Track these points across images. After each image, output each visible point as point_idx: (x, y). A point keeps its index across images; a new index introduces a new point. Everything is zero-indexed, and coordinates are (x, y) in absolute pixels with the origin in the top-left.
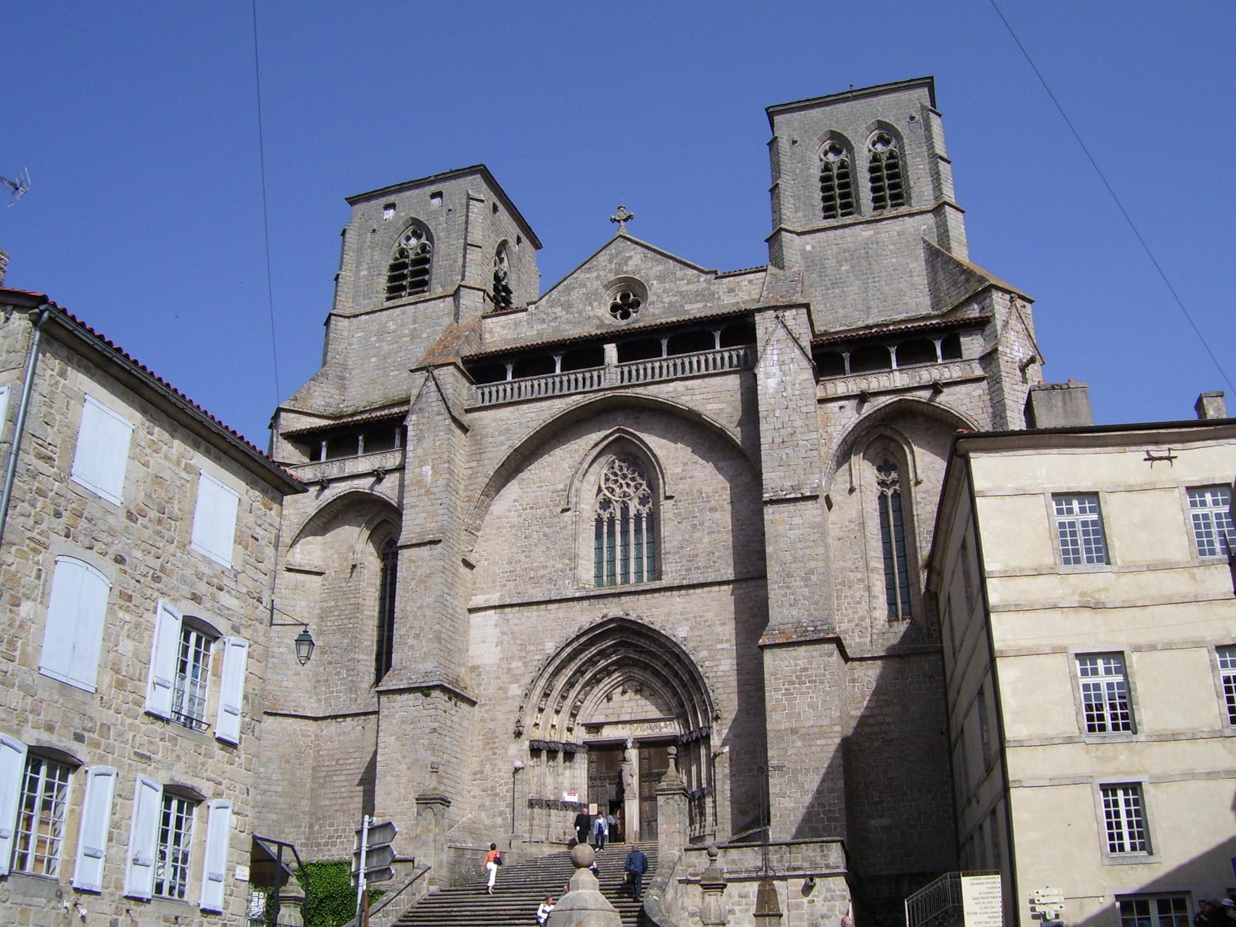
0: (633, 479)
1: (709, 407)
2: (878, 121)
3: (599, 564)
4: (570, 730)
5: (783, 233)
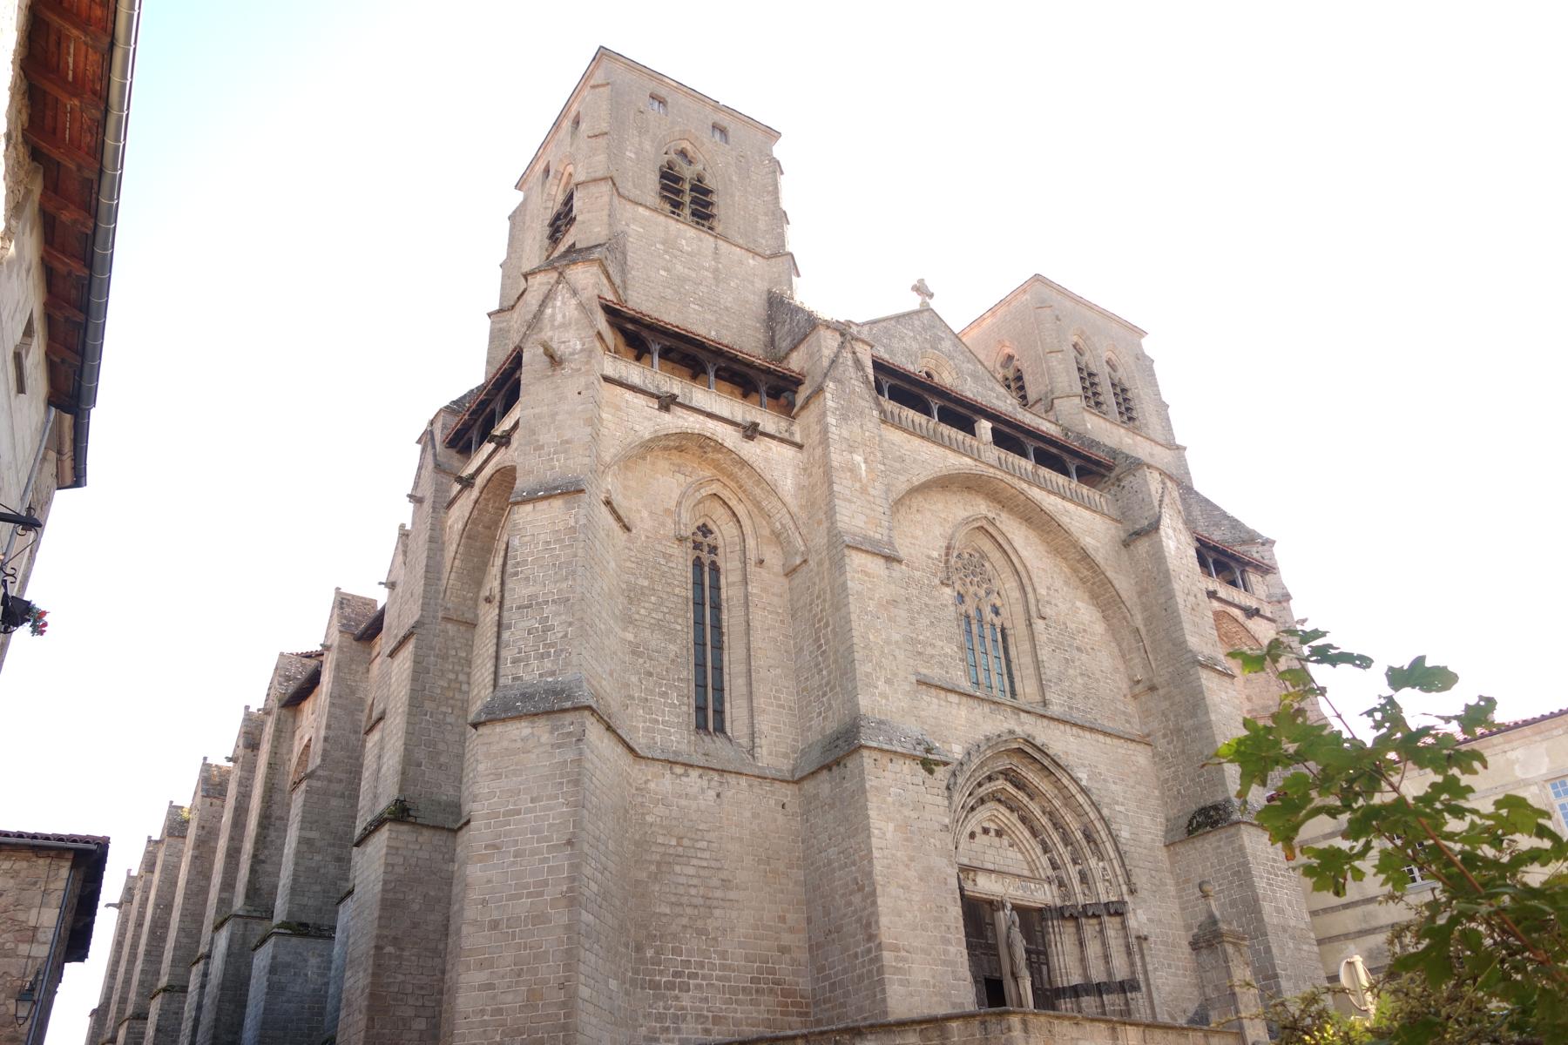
1: (1088, 539)
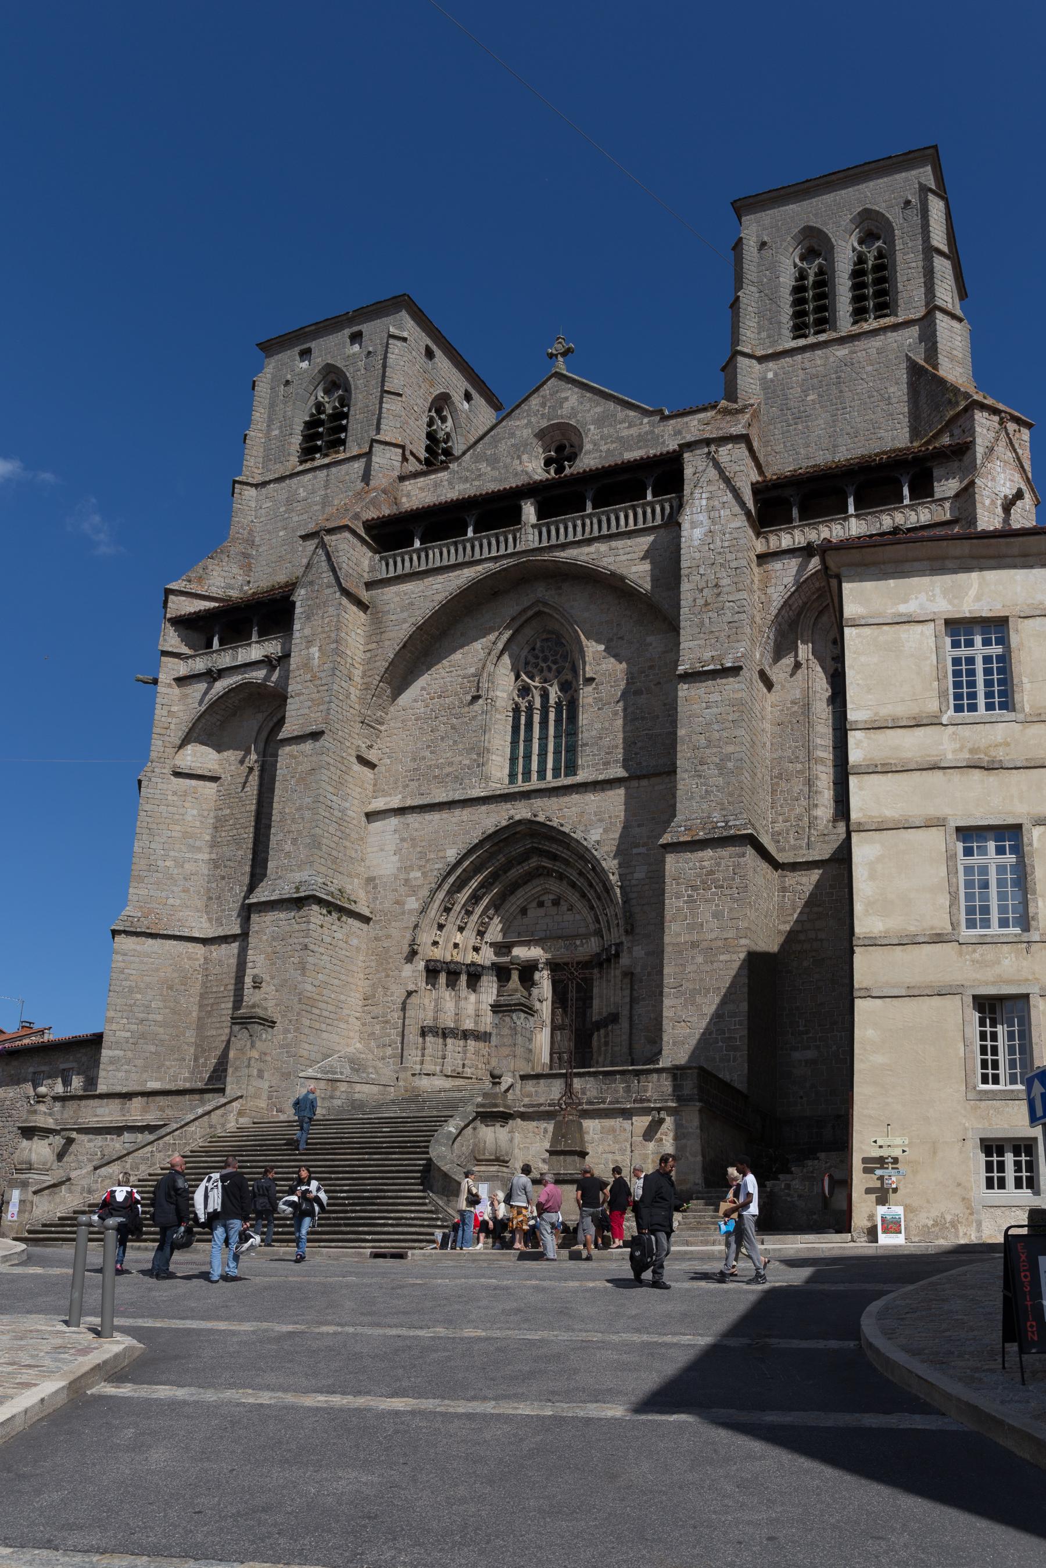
0: (555, 662)
1: (634, 569)
2: (867, 211)
3: (513, 760)
4: (476, 949)
5: (740, 359)
